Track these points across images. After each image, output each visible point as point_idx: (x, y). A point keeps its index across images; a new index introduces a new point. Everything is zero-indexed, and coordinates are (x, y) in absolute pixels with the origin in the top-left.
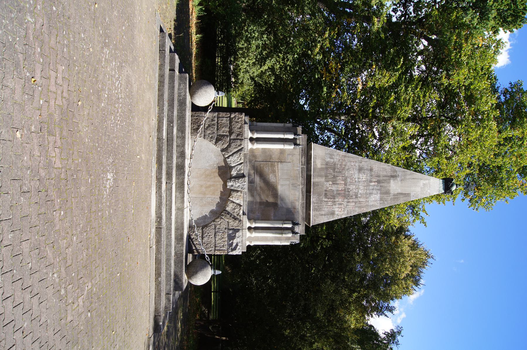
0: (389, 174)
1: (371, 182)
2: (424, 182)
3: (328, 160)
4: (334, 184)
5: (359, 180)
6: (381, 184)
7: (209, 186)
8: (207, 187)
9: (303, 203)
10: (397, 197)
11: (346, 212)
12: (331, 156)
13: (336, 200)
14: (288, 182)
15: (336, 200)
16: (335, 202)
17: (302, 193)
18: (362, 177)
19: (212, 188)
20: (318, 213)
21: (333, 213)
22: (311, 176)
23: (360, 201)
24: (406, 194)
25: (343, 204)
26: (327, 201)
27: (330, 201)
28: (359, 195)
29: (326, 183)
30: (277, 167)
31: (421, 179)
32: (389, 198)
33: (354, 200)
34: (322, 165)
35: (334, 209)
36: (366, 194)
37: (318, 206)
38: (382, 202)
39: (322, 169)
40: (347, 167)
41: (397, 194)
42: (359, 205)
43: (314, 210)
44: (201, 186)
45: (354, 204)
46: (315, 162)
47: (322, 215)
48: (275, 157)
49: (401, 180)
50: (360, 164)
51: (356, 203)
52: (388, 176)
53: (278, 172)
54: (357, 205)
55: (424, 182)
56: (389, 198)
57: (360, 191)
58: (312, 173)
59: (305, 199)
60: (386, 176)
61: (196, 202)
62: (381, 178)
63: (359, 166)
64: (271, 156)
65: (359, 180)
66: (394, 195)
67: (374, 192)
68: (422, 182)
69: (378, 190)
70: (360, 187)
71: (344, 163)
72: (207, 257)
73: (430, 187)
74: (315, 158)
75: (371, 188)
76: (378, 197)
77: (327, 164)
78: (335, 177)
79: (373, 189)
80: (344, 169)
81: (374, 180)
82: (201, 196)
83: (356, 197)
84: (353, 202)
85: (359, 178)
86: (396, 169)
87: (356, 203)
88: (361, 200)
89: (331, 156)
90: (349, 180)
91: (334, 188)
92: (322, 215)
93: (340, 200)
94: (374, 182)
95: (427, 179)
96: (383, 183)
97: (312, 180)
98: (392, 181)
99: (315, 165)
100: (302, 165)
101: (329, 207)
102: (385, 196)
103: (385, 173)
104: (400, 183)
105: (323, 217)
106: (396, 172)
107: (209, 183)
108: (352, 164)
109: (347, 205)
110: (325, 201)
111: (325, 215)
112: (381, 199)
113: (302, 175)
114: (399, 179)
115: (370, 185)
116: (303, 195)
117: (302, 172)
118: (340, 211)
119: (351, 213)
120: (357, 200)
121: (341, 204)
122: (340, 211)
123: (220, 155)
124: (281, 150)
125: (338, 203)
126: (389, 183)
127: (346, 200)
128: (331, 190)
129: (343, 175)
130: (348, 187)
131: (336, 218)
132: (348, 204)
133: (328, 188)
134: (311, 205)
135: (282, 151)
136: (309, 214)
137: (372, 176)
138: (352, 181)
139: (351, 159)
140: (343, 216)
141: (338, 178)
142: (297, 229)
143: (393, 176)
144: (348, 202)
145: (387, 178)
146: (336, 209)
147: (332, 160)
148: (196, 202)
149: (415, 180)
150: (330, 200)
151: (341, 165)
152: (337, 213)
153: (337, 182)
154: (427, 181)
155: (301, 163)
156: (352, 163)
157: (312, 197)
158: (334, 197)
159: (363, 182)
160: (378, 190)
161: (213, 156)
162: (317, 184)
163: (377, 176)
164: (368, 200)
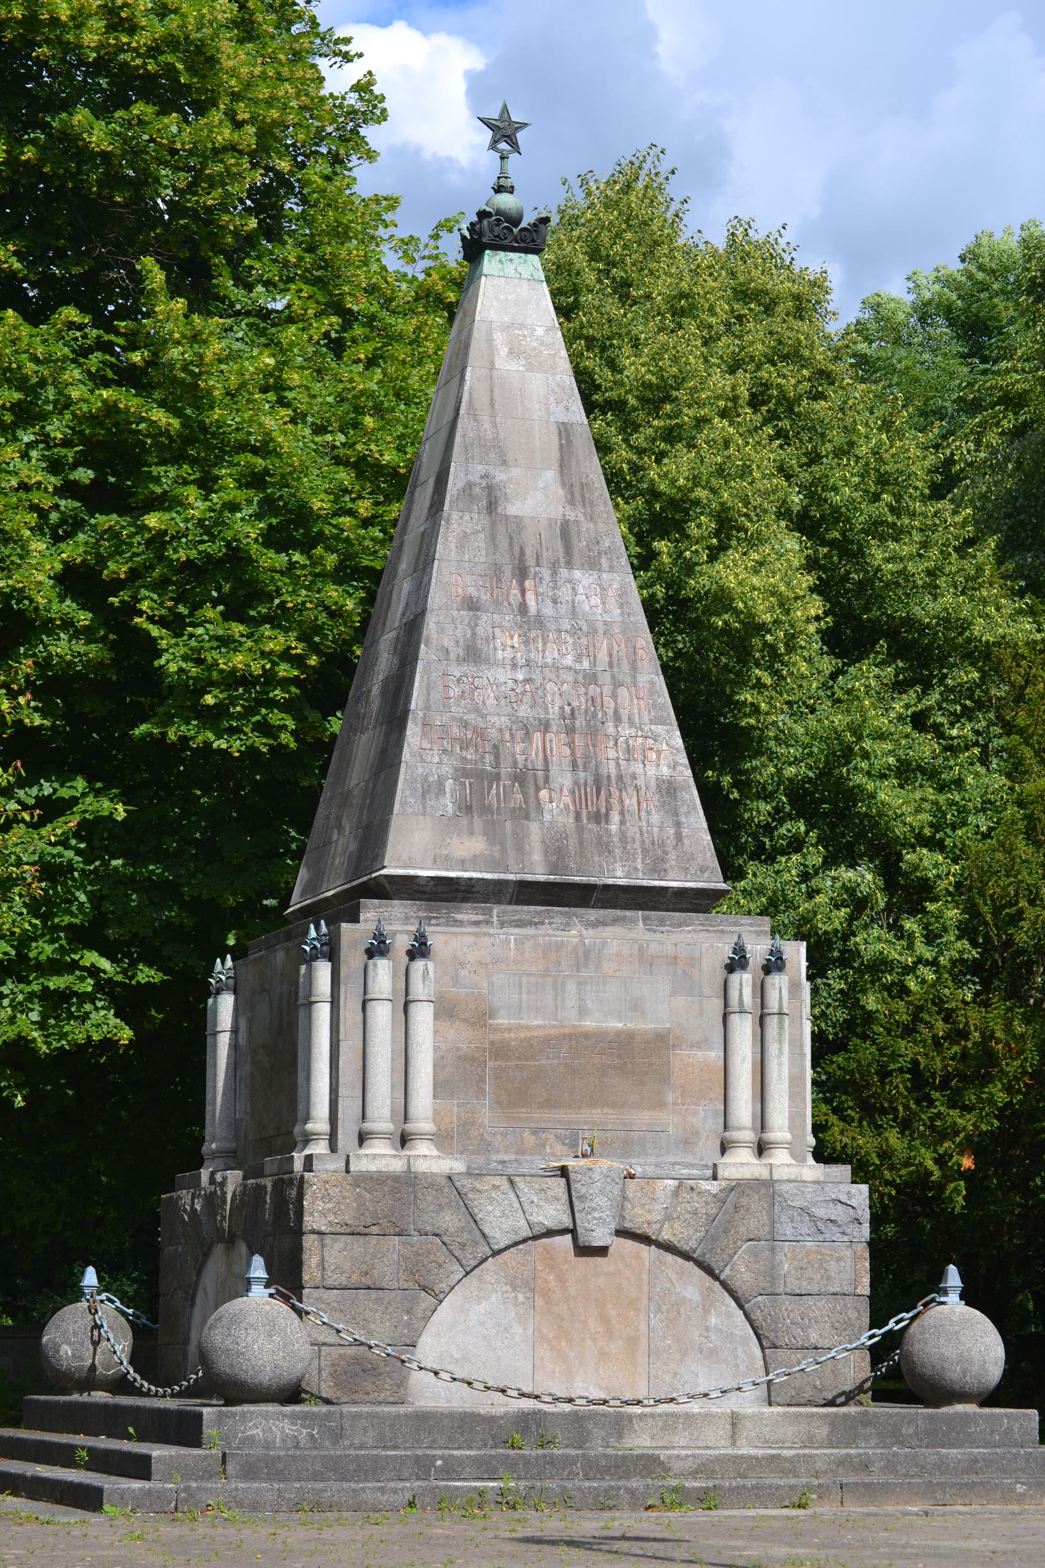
0: (485, 520)
1: (523, 608)
2: (503, 351)
3: (448, 804)
4: (547, 780)
5: (521, 661)
6: (530, 561)
7: (604, 1319)
8: (609, 1332)
9: (645, 919)
10: (577, 490)
11: (659, 729)
12: (431, 789)
13: (613, 772)
14: (571, 987)
15: (613, 772)
16: (620, 778)
17: (604, 924)
18: (508, 654)
19: (611, 1311)
20: (672, 856)
21: (668, 789)
22: (522, 884)
23: (611, 665)
24: (561, 446)
25: (627, 742)
26: (622, 813)
27: (622, 802)
28: (586, 664)
29: (547, 817)
30: (509, 1030)
31: (492, 367)
32: (586, 525)
33: (607, 690)
34: (471, 833)
35: (653, 783)
36: (575, 631)
37: (645, 852)
38: (603, 560)
39: (492, 833)
40: (471, 717)
41: (563, 485)
42: (626, 666)
43: (662, 874)
44: (603, 1355)
45: (623, 692)
46: (463, 861)
47: (679, 837)
48: (462, 1037)
49: (504, 463)
50: (452, 656)
51: (616, 684)
52: (493, 525)
53: (528, 1028)
54: (629, 680)
55: (503, 351)
56: (586, 525)
57: (569, 661)
58: (511, 877)
59: (628, 913)
60: (493, 537)
61: (668, 1378)
62: (505, 559)
63: (459, 661)
64: (464, 1058)
65: (521, 661)
66: (572, 502)
67: (565, 593)
68: (504, 363)
69: (554, 574)
70: (549, 660)
71: (456, 731)
72: (897, 1323)
73: (522, 326)
74: (446, 861)
75: (548, 610)
76: (584, 579)
77: (469, 809)
78: (520, 778)
79: (555, 602)
80: (481, 733)
81: (515, 592)
82: (642, 1358)
83: (592, 678)
84: (614, 696)
85: (514, 666)
86: (460, 485)
87: (616, 684)
88: (603, 656)
89: (431, 789)
90: (524, 711)
91: (563, 778)
92: (679, 837)
93: (612, 754)
94: (523, 592)
95: (490, 341)
96: (522, 553)
97: (542, 878)
98: (513, 509)
99: (474, 862)
100: (488, 923)
101: (644, 805)
102: (580, 545)
103: (481, 541)
104: (515, 472)
105: (685, 831)
106: (470, 485)
107: (593, 1324)
108: (454, 691)
109: (631, 723)
110: (622, 822)
111: (678, 825)
112: (592, 565)
113: (531, 923)
114: (500, 476)
115: (538, 616)
116: (615, 921)
117: (520, 924)
118: (659, 753)
119: (663, 707)
120: (607, 677)
121: (628, 750)
122: (659, 753)
123: (480, 1279)
124: (790, 1044)
125: (623, 763)
126: (519, 521)
127: (610, 728)
128: (573, 792)
129: (507, 736)
130: (554, 711)
131: (685, 773)
132: (625, 718)
133: (567, 806)
134: (645, 883)
135: (445, 1010)
136: (681, 892)
137: (497, 604)
138: (527, 698)
139: (436, 696)
140: (678, 741)
141: (520, 759)
142: (758, 949)
143: (492, 506)
144: (617, 718)
145: (501, 529)
146: (652, 771)
147: (449, 784)
148: (668, 1378)
149: (496, 397)
150: (615, 802)
151: (465, 745)
152: (665, 771)
153: (540, 764)
154: (499, 337)
155: (485, 929)
156: (451, 694)
157: (610, 881)
158: (599, 782)
159: (526, 643)
160: (554, 574)
161: (483, 1307)
162: (556, 854)
163: (499, 580)
164: (601, 628)
